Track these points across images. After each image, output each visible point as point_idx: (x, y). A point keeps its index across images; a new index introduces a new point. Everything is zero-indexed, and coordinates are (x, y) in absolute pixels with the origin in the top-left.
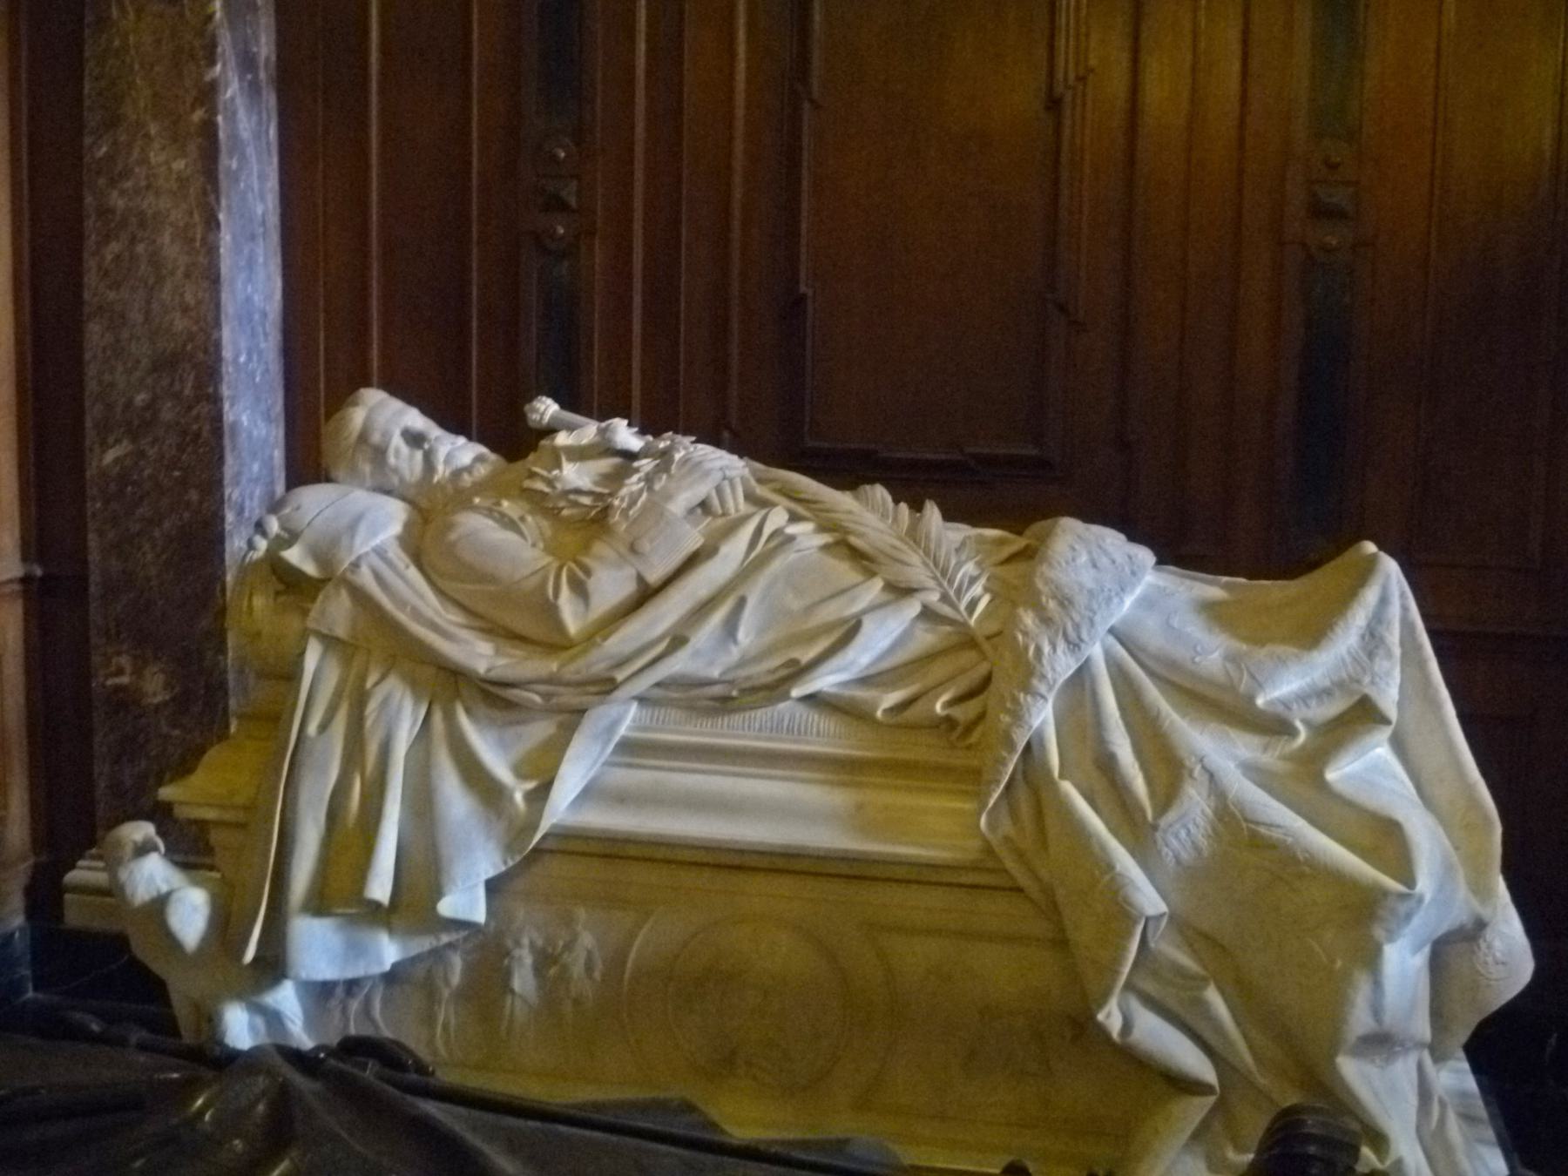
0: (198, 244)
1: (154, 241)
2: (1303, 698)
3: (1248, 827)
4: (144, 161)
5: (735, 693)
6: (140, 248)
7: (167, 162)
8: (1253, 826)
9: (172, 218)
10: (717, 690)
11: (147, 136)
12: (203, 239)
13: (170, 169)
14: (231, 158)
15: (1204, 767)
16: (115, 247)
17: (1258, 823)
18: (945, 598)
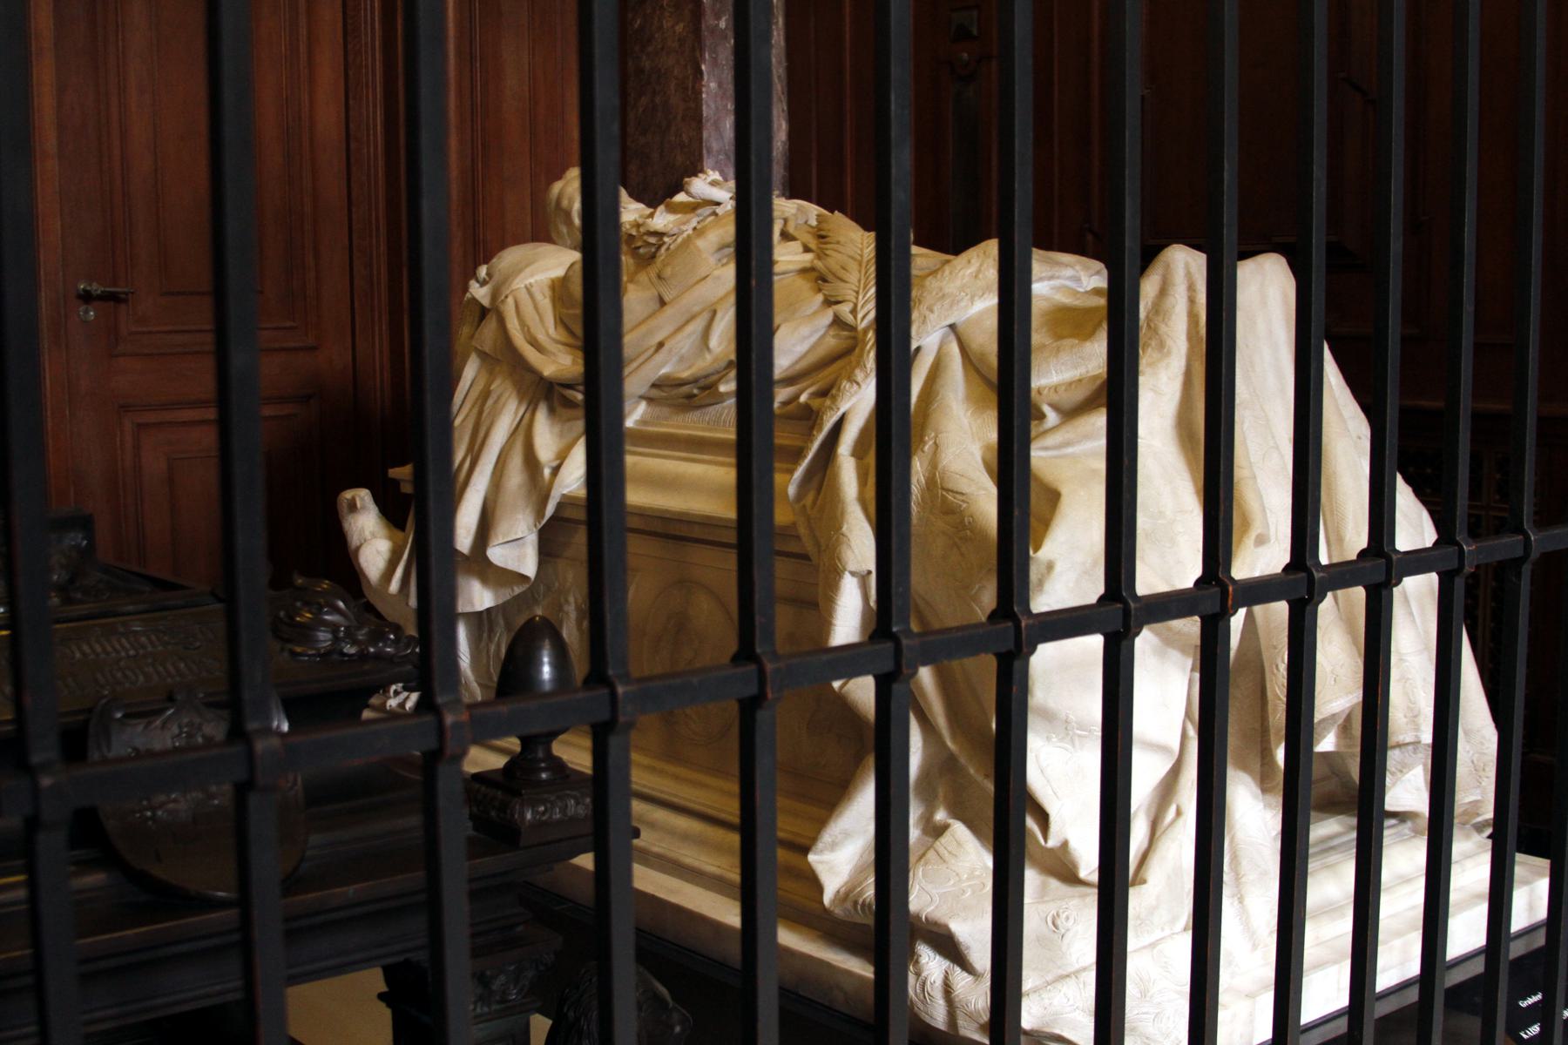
0: (690, 93)
1: (665, 93)
2: (1056, 388)
3: (942, 495)
4: (661, 27)
5: (695, 391)
6: (658, 100)
7: (673, 27)
8: (944, 493)
9: (676, 72)
10: (685, 389)
11: (662, 6)
12: (693, 87)
13: (674, 32)
14: (718, 18)
15: (935, 443)
16: (644, 100)
17: (948, 490)
18: (854, 312)
